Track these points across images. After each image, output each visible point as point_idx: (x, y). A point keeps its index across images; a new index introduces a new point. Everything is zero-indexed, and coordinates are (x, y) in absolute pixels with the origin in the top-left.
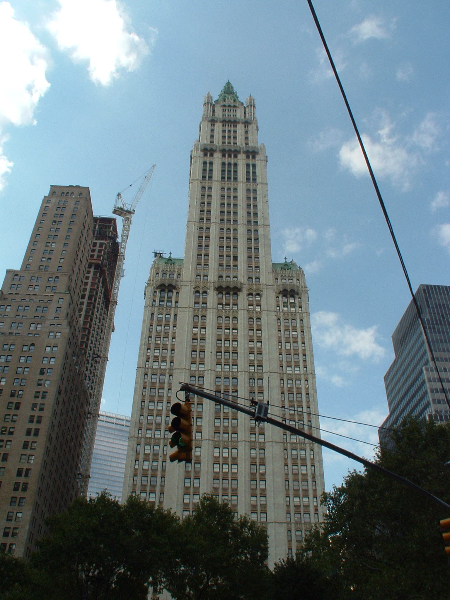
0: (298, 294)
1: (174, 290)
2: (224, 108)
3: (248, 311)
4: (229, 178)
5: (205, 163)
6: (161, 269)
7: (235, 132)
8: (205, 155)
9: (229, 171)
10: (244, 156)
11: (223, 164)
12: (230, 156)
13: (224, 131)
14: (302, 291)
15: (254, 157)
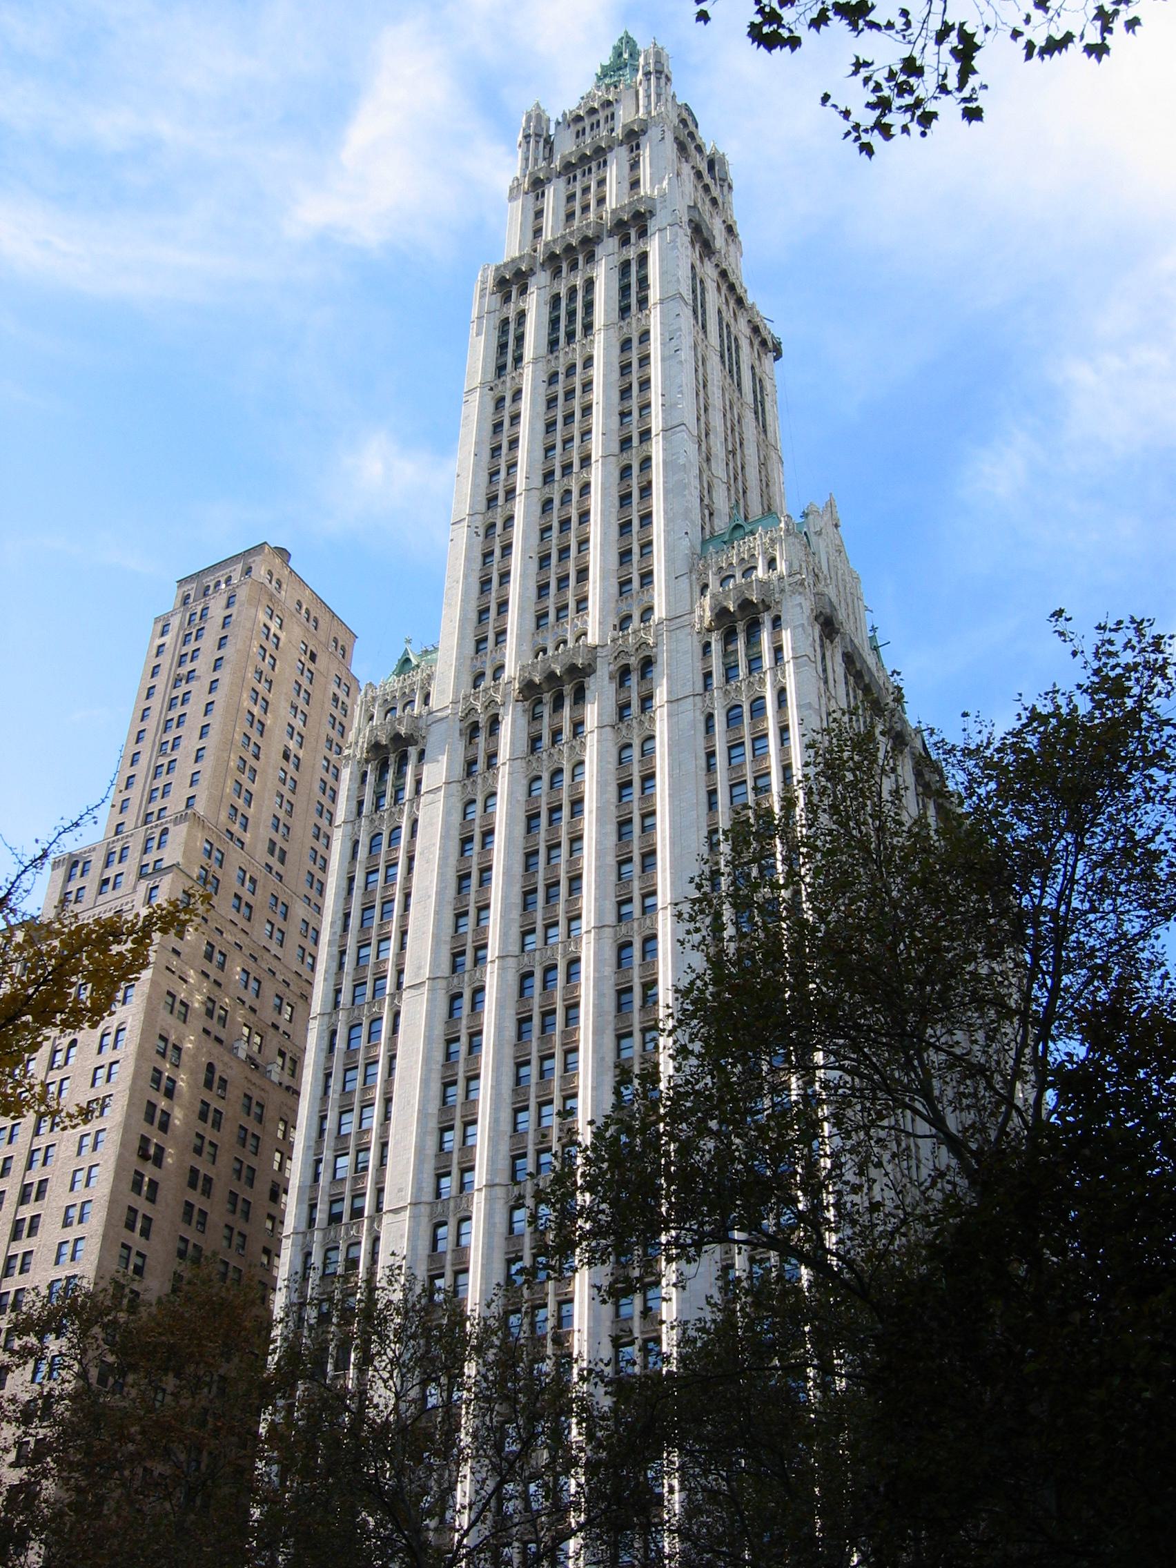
0: (768, 608)
1: (410, 748)
2: (579, 126)
3: (613, 727)
4: (571, 336)
5: (505, 322)
6: (379, 702)
7: (602, 182)
8: (507, 299)
9: (572, 314)
10: (611, 244)
11: (556, 299)
12: (574, 267)
13: (571, 198)
14: (782, 591)
15: (643, 233)
